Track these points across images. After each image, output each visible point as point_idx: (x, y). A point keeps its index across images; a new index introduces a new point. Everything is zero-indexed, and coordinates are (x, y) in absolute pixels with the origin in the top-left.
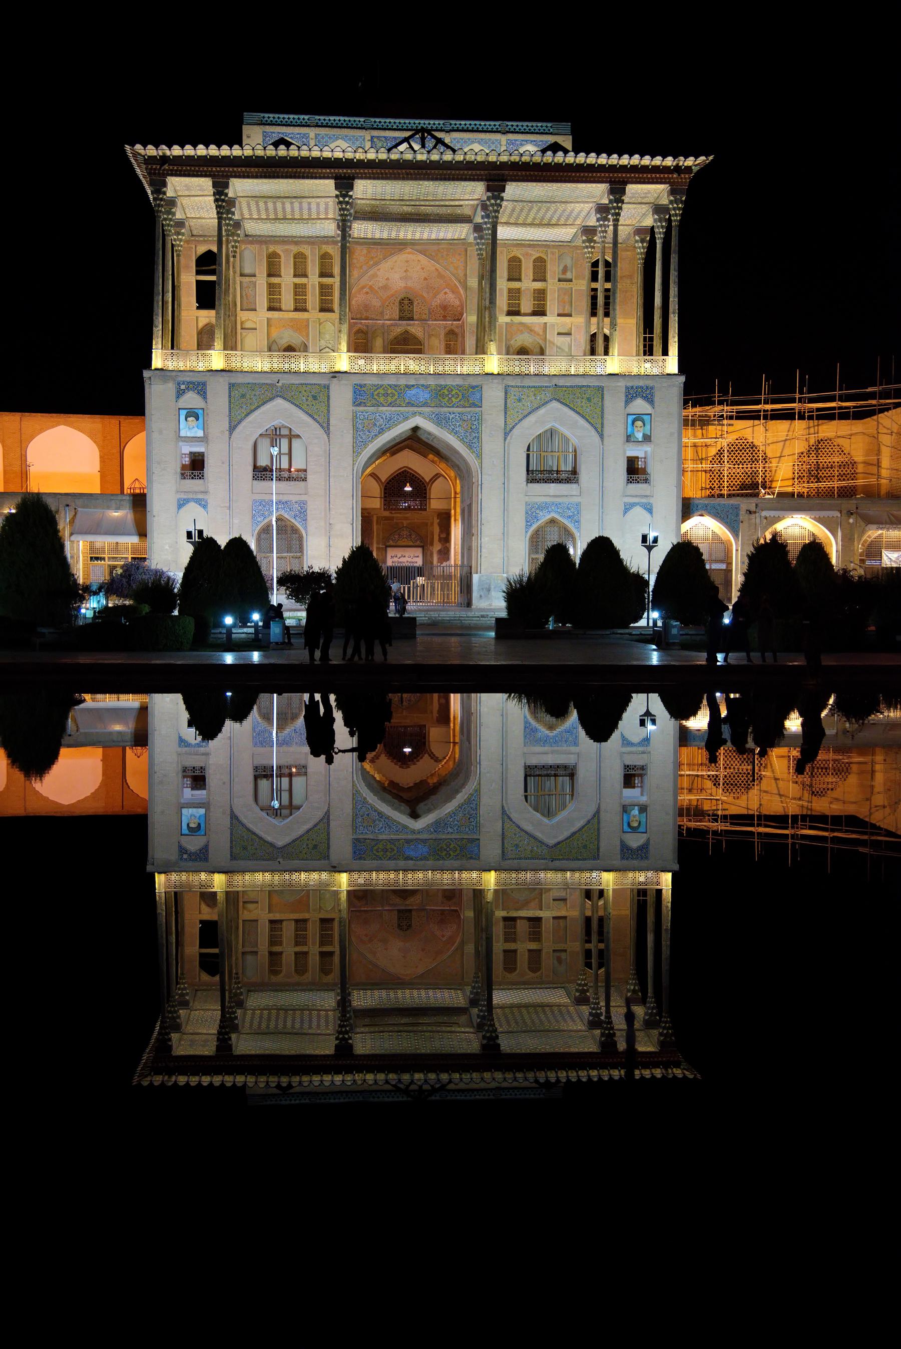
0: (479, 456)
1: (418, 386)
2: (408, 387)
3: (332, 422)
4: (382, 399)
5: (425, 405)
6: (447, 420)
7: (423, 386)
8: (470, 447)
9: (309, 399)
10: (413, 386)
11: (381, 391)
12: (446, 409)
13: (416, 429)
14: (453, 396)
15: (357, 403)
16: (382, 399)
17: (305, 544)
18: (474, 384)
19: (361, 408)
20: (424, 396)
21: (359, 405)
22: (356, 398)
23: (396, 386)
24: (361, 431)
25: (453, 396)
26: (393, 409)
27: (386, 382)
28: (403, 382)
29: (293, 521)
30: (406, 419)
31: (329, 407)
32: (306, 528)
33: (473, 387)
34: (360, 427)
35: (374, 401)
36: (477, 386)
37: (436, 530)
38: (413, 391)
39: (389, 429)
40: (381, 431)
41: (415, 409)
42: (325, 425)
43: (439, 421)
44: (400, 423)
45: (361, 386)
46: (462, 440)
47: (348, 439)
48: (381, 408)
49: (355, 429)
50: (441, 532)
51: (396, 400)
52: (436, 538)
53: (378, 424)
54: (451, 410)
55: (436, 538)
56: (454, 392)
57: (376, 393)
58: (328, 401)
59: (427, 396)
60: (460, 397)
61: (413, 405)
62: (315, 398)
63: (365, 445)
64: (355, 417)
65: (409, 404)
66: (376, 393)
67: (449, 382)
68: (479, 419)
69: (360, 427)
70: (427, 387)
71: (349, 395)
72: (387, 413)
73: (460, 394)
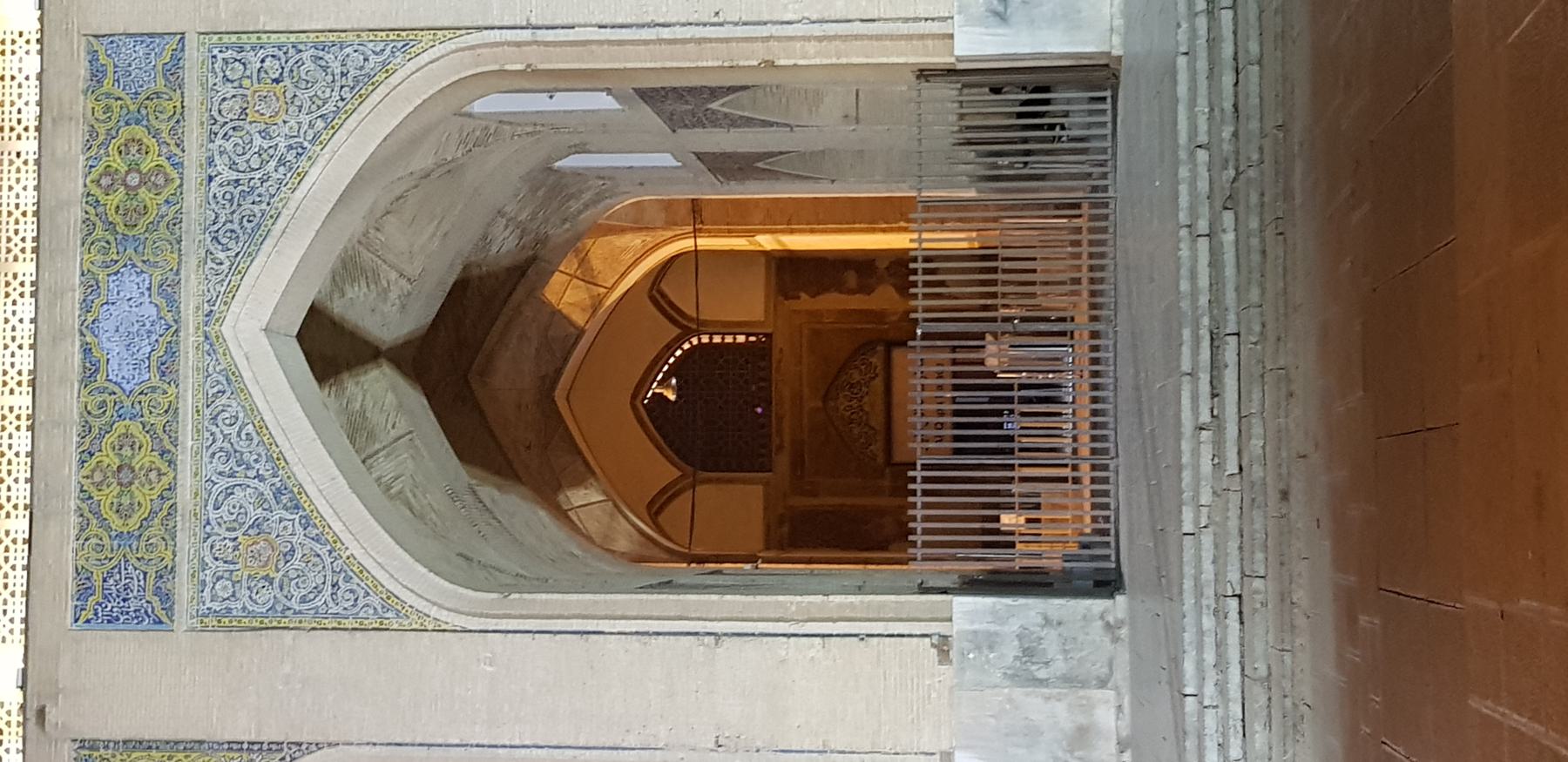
0: (403, 38)
1: (89, 327)
2: (91, 370)
4: (144, 495)
5: (169, 292)
6: (240, 190)
7: (86, 307)
8: (360, 85)
10: (87, 350)
11: (108, 496)
12: (192, 199)
13: (328, 346)
14: (133, 168)
15: (154, 613)
16: (144, 495)
18: (83, 71)
19: (183, 590)
20: (131, 298)
21: (166, 598)
22: (139, 615)
23: (87, 429)
24: (295, 592)
25: (133, 168)
26: (188, 440)
27: (70, 475)
28: (69, 401)
30: (232, 377)
33: (97, 75)
34: (265, 596)
35: (156, 529)
36: (93, 56)
37: (832, 301)
38: (111, 346)
39: (277, 461)
40: (290, 497)
41: (190, 339)
43: (243, 226)
44: (253, 410)
45: (84, 592)
46: (332, 123)
47: (318, 654)
48: (185, 496)
49: (272, 621)
50: (841, 288)
51: (148, 429)
52: (857, 302)
53: (255, 513)
54: (193, 174)
55: (857, 302)
56: (119, 164)
57: (116, 523)
59: (131, 284)
60: (139, 131)
61: (172, 351)
63: (345, 573)
64: (221, 620)
65: (167, 368)
66: (116, 523)
67: (74, 184)
68: (235, 45)
69: (265, 596)
70: (92, 286)
71: (123, 650)
72: (209, 470)
73: (125, 134)
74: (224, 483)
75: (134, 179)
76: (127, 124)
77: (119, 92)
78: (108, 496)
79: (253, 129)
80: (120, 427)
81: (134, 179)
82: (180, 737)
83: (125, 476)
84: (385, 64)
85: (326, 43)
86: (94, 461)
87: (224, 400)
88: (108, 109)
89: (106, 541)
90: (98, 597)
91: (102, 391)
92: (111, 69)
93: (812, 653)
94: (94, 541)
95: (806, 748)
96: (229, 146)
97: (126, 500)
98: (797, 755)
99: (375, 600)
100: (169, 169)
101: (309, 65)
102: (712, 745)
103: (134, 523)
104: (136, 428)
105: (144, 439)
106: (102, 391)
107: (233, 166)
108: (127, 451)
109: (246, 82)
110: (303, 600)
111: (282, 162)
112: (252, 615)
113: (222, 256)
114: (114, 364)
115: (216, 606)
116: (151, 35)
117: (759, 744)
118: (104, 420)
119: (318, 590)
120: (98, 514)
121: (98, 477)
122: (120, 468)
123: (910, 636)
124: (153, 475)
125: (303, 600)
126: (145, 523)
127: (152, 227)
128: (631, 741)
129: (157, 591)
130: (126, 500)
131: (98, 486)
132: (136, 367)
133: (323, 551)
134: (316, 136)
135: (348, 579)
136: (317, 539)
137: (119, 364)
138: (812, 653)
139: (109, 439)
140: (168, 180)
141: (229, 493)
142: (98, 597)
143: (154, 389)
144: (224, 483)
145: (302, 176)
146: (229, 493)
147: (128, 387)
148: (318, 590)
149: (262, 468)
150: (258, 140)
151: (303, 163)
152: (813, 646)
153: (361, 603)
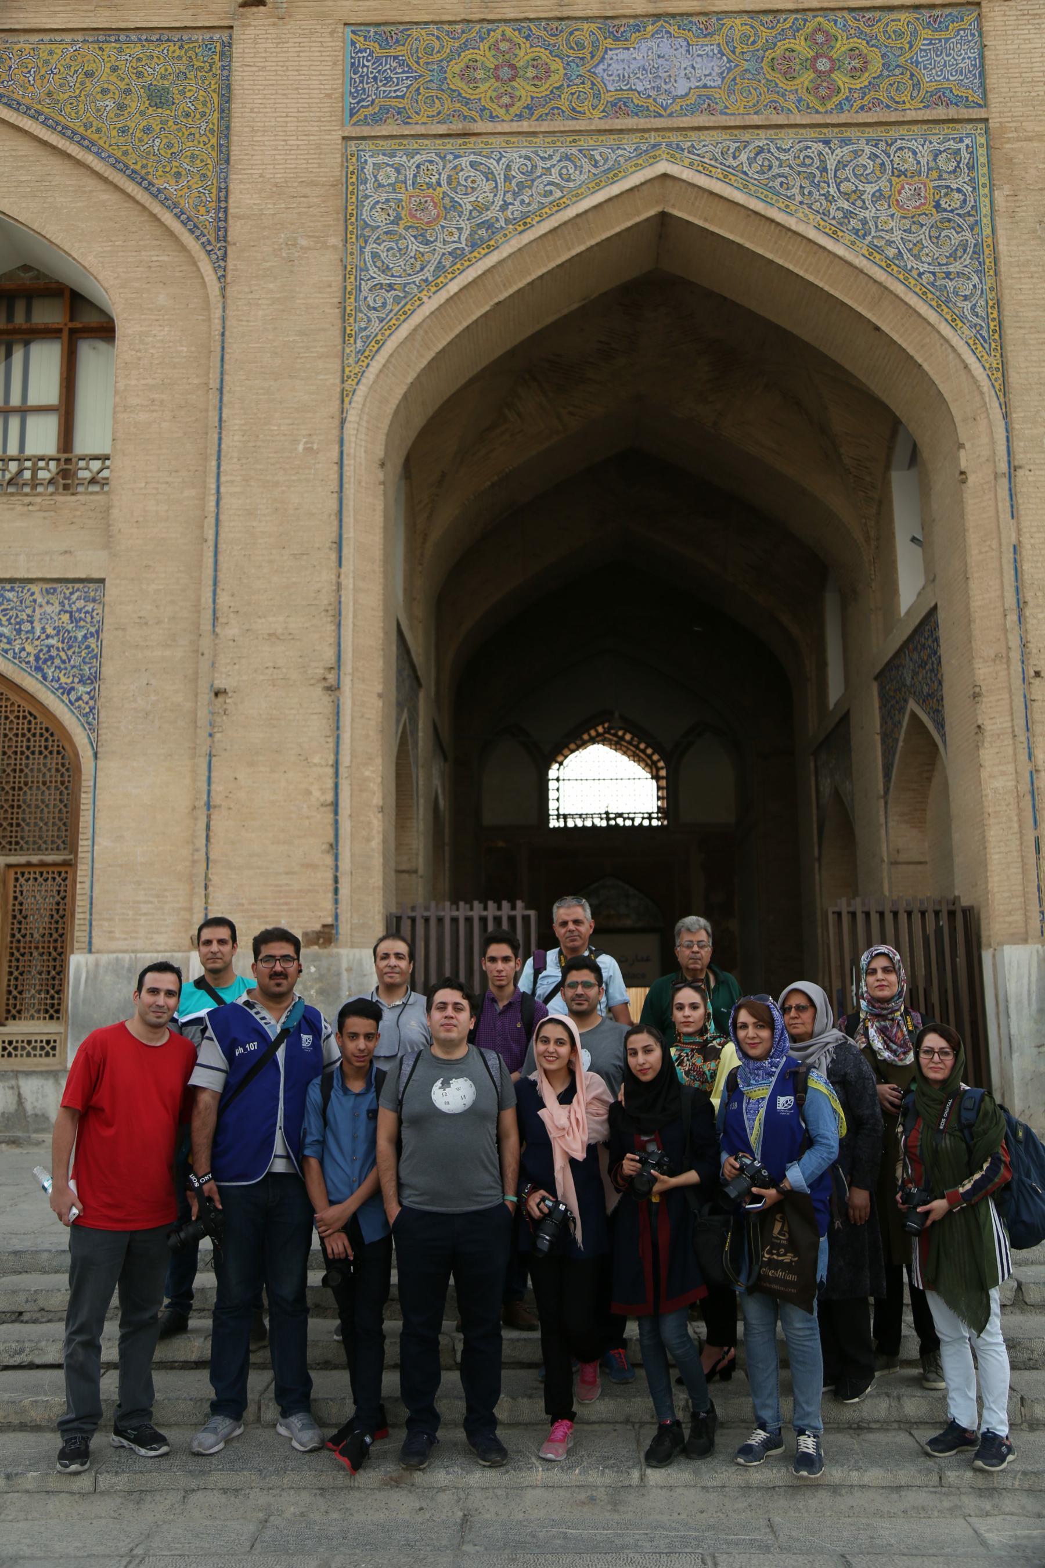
3: (243, 198)
9: (133, 105)
16: (487, 89)
17: (85, 798)
22: (357, 94)
29: (30, 683)
31: (225, 131)
32: (91, 719)
34: (380, 218)
35: (448, 106)
42: (206, 218)
47: (320, 272)
49: (353, 226)
51: (556, 92)
53: (467, 203)
56: (841, 47)
58: (225, 112)
60: (876, 65)
62: (159, 98)
64: (352, 177)
69: (380, 218)
74: (498, 170)
75: (823, 65)
76: (884, 56)
77: (920, 44)
78: (484, 55)
79: (883, 183)
80: (556, 65)
81: (823, 65)
82: (234, 139)
83: (505, 72)
84: (962, 318)
85: (985, 258)
86: (521, 40)
87: (587, 166)
88: (900, 35)
89: (437, 57)
90: (378, 52)
91: (595, 45)
92: (943, 35)
93: (317, 793)
94: (437, 44)
95: (213, 787)
96: (863, 160)
97: (480, 74)
98: (205, 778)
99: (375, 326)
100: (836, 100)
101: (956, 239)
102: (220, 683)
103: (459, 84)
104: (555, 79)
105: (544, 89)
106: (595, 45)
107: (841, 165)
108: (531, 73)
109: (935, 174)
110: (375, 255)
111: (848, 215)
112: (360, 205)
113: (743, 157)
114: (624, 55)
115: (369, 168)
116: (982, 75)
117: (218, 736)
118: (565, 50)
119: (385, 270)
120: (464, 47)
121: (504, 46)
122: (513, 67)
123: (336, 902)
124: (506, 100)
125: (375, 255)
126: (455, 95)
127: (772, 86)
128: (223, 599)
129: (385, 110)
130: (480, 74)
131: (495, 46)
132: (622, 78)
133: (427, 274)
134: (879, 250)
135: (397, 300)
136: (440, 267)
137: (624, 65)
138: (317, 793)
139: (544, 54)
140: (823, 99)
141: (489, 175)
142: (378, 52)
143: (597, 96)
144: (498, 170)
145: (834, 236)
146: (489, 175)
147: (599, 69)
148: (385, 270)
149: (516, 209)
150: (870, 189)
151: (849, 237)
152: (323, 791)
153: (373, 315)
